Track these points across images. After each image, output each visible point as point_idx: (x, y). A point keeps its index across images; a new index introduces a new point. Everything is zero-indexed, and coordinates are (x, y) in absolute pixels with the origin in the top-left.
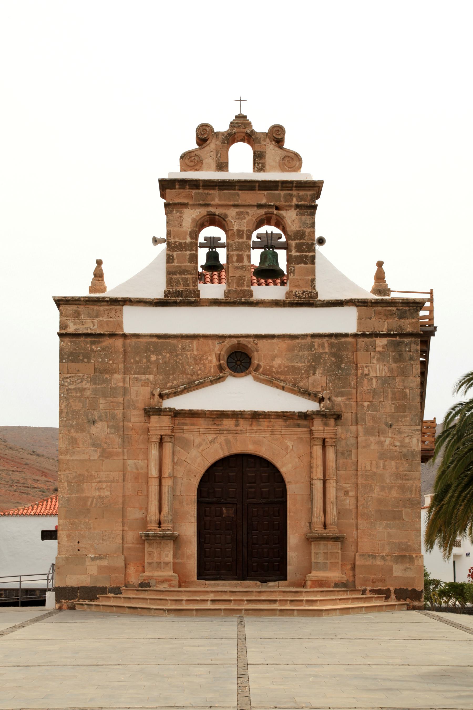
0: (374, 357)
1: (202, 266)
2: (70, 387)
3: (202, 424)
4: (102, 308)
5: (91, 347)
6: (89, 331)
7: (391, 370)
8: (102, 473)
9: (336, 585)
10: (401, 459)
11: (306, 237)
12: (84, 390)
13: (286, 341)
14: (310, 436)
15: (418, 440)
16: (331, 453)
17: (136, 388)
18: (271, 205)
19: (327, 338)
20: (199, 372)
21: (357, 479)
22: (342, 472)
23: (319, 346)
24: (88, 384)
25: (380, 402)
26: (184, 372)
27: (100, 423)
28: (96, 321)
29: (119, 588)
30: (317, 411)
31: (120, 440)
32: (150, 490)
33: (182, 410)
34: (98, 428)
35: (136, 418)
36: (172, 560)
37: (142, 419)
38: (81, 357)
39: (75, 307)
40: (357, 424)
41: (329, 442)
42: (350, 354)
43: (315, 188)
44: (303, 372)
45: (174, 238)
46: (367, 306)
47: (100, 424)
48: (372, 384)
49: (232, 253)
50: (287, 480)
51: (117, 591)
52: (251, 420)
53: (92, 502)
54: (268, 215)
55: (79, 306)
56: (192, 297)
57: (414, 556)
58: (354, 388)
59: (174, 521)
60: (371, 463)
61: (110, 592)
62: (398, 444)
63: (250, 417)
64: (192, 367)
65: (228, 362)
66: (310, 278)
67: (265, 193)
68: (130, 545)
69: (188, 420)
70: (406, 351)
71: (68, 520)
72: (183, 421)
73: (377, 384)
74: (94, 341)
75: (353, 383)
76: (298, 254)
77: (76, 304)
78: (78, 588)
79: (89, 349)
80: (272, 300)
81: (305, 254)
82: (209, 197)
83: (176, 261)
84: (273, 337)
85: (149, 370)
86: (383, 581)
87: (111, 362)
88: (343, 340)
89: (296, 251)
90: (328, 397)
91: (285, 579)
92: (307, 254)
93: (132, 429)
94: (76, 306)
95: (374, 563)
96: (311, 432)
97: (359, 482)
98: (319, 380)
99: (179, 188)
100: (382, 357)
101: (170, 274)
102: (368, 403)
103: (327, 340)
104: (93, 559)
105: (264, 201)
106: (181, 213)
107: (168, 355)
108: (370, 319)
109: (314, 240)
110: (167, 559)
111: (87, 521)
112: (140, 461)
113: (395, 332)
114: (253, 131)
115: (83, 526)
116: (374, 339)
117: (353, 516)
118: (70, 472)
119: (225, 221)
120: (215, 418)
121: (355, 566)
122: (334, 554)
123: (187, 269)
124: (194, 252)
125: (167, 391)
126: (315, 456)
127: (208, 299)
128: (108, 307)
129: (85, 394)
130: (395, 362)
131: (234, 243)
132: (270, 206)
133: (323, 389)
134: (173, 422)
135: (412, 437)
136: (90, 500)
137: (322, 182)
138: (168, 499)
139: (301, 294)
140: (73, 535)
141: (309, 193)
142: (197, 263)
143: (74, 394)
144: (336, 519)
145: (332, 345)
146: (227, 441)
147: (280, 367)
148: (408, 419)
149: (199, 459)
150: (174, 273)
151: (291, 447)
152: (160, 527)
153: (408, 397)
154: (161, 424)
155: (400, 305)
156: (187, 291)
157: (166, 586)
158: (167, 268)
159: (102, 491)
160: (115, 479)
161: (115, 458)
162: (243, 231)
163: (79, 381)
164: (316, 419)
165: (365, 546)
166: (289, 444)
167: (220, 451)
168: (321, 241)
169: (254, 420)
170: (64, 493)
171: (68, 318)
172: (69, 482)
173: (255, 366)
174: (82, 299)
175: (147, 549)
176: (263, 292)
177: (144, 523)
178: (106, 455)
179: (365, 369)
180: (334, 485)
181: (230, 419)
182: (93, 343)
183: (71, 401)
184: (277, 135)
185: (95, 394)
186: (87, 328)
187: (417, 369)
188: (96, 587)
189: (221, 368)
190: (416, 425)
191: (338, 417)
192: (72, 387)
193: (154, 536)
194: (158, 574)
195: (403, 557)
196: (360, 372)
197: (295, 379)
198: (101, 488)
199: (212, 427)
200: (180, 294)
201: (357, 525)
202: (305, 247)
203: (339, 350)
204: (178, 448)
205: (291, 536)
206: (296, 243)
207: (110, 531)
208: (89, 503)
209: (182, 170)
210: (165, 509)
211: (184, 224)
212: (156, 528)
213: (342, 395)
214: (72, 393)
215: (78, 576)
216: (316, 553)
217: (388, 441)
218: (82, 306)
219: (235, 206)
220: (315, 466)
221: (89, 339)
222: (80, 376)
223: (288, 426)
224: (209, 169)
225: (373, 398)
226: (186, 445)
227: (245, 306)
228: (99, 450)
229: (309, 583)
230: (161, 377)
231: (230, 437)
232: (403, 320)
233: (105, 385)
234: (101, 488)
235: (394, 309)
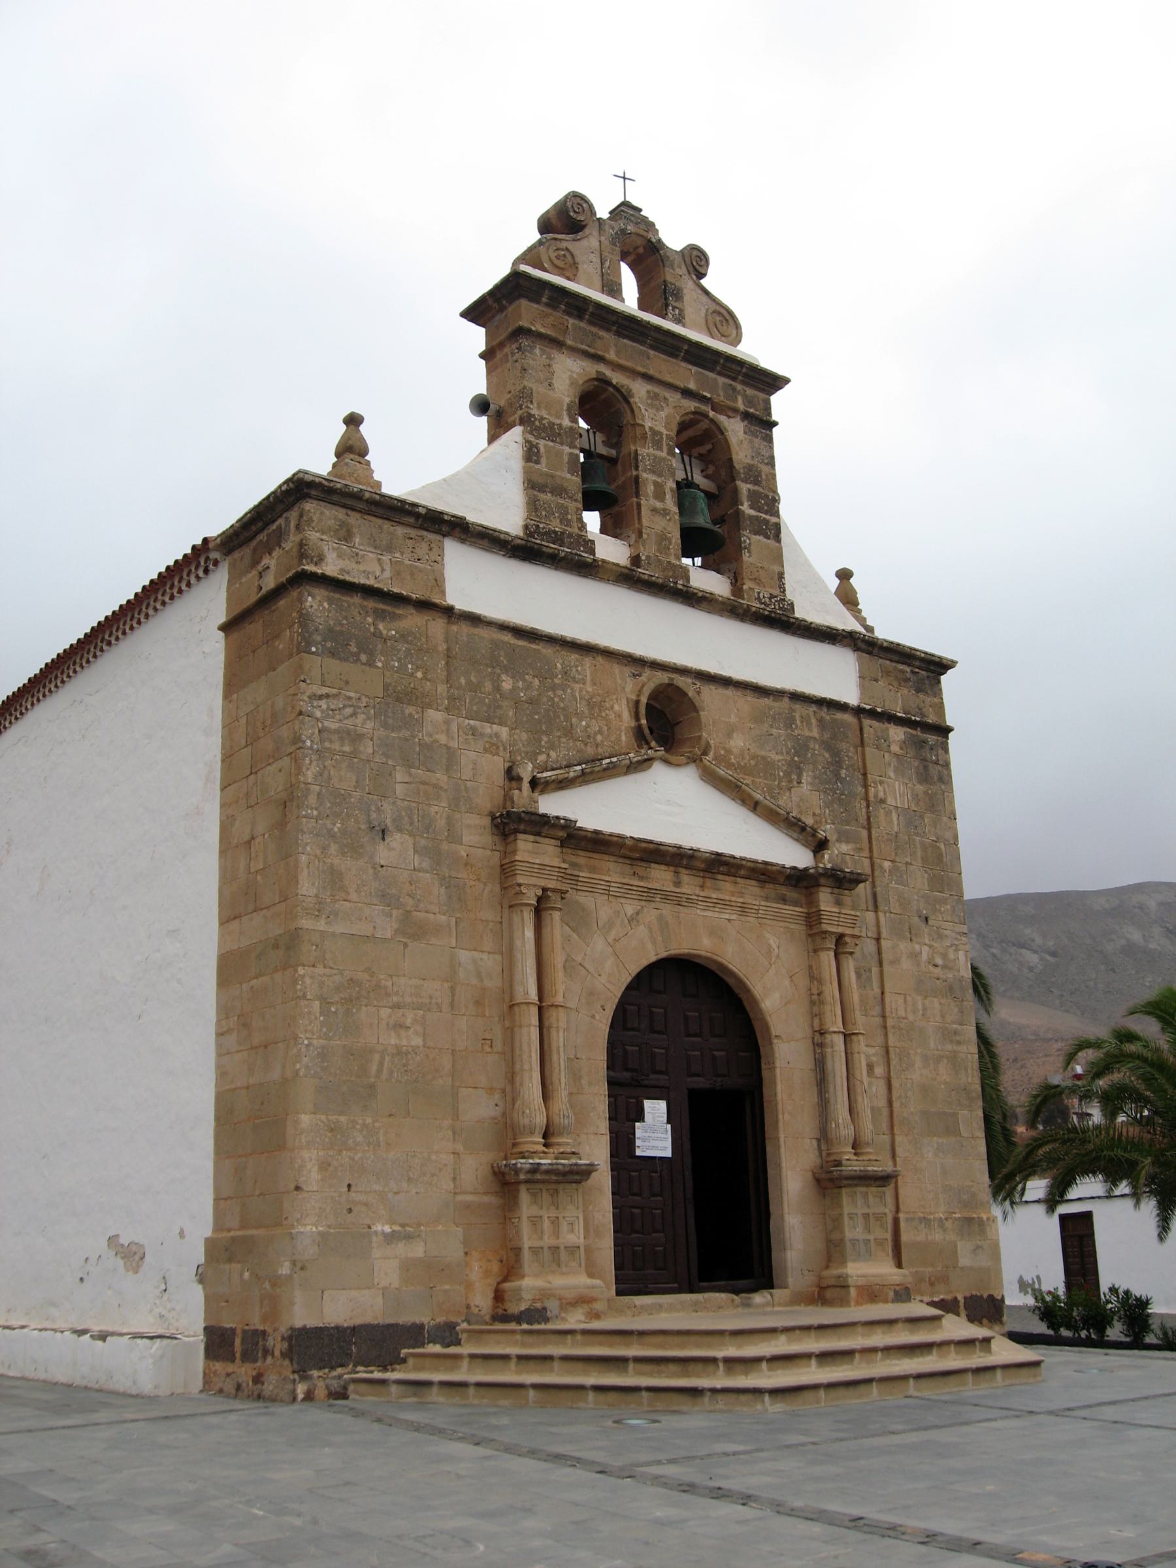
2: (326, 724)
3: (612, 871)
4: (400, 531)
5: (376, 628)
6: (371, 582)
7: (916, 797)
8: (402, 980)
13: (749, 699)
18: (705, 397)
19: (814, 708)
20: (599, 738)
21: (886, 1035)
24: (370, 725)
26: (569, 732)
27: (398, 836)
28: (386, 558)
29: (451, 1327)
31: (443, 890)
34: (393, 849)
35: (475, 836)
39: (340, 513)
40: (876, 909)
45: (539, 407)
46: (870, 653)
47: (397, 840)
49: (645, 475)
51: (448, 1334)
53: (381, 1064)
55: (350, 512)
57: (985, 1218)
61: (433, 1341)
62: (939, 961)
67: (694, 369)
68: (469, 1198)
71: (323, 1117)
73: (898, 824)
74: (383, 611)
76: (753, 512)
77: (344, 506)
78: (354, 1329)
82: (599, 341)
83: (544, 461)
84: (726, 682)
85: (499, 712)
86: (945, 1279)
92: (767, 517)
93: (466, 864)
94: (344, 511)
95: (930, 1238)
97: (890, 1044)
98: (804, 797)
99: (547, 305)
104: (390, 1238)
105: (692, 386)
107: (536, 682)
108: (876, 680)
111: (369, 1121)
112: (485, 956)
115: (360, 1139)
118: (327, 970)
119: (628, 402)
123: (566, 484)
128: (413, 533)
129: (362, 748)
130: (920, 782)
131: (648, 455)
132: (703, 399)
135: (956, 950)
136: (377, 1057)
140: (335, 1163)
143: (336, 746)
147: (742, 755)
158: (527, 473)
159: (403, 1033)
160: (434, 1001)
161: (433, 941)
162: (661, 434)
163: (349, 711)
166: (771, 942)
167: (650, 946)
169: (708, 875)
170: (312, 1032)
171: (324, 537)
172: (325, 1002)
178: (413, 930)
181: (663, 867)
182: (380, 615)
183: (328, 763)
185: (384, 754)
186: (367, 574)
188: (397, 1325)
189: (640, 737)
192: (334, 726)
195: (969, 1220)
196: (872, 791)
198: (401, 1026)
200: (558, 538)
203: (834, 737)
205: (789, 1173)
207: (425, 1155)
208: (374, 1068)
211: (557, 383)
213: (847, 842)
214: (331, 741)
215: (354, 1293)
217: (925, 953)
218: (358, 515)
219: (648, 378)
221: (371, 604)
222: (350, 698)
223: (767, 899)
226: (580, 922)
227: (676, 600)
228: (395, 912)
230: (524, 736)
231: (667, 910)
232: (921, 696)
234: (401, 1026)
235: (908, 669)
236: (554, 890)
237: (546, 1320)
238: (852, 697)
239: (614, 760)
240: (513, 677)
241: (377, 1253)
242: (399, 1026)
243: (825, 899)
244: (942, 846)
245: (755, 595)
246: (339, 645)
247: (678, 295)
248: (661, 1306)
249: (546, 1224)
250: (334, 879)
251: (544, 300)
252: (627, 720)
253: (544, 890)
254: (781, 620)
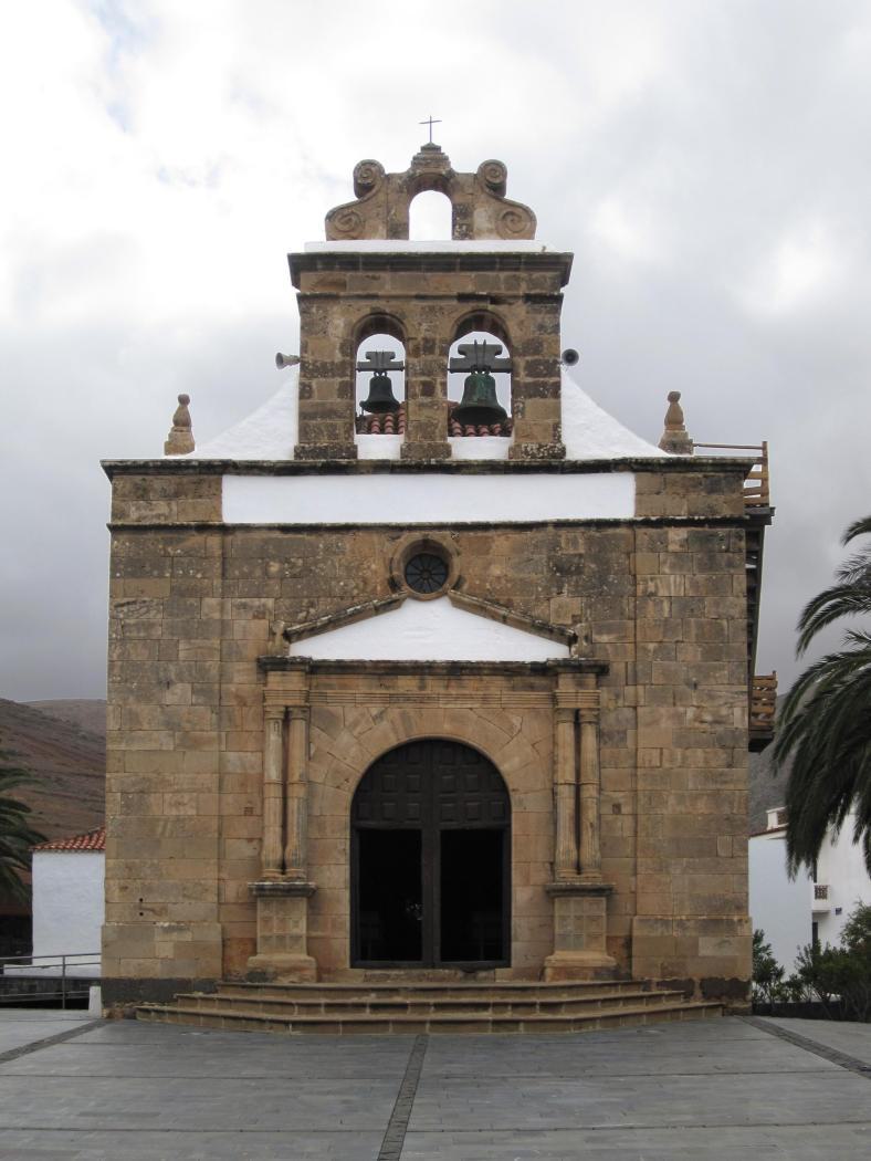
0: (665, 562)
1: (362, 404)
2: (127, 621)
3: (361, 686)
6: (162, 521)
7: (695, 585)
8: (182, 776)
10: (714, 746)
11: (545, 351)
12: (152, 625)
14: (551, 706)
15: (743, 711)
17: (243, 622)
18: (482, 296)
19: (582, 529)
22: (608, 771)
23: (567, 543)
24: (160, 616)
25: (677, 642)
27: (180, 685)
30: (565, 660)
32: (267, 805)
33: (324, 661)
35: (242, 677)
36: (304, 932)
37: (254, 677)
38: (148, 568)
41: (587, 716)
42: (623, 556)
43: (558, 266)
44: (540, 589)
45: (313, 354)
47: (179, 688)
48: (662, 609)
49: (414, 379)
50: (511, 787)
51: (209, 986)
52: (446, 677)
53: (165, 827)
54: (478, 313)
56: (344, 458)
57: (736, 918)
58: (630, 619)
59: (308, 863)
60: (661, 754)
62: (708, 718)
63: (445, 671)
64: (342, 584)
65: (406, 574)
66: (550, 421)
67: (473, 274)
69: (334, 680)
70: (721, 551)
72: (327, 681)
73: (671, 611)
74: (171, 538)
75: (628, 609)
76: (529, 380)
78: (142, 981)
79: (162, 552)
80: (485, 461)
81: (542, 379)
85: (266, 589)
87: (199, 576)
88: (610, 531)
89: (527, 375)
90: (584, 633)
91: (509, 966)
92: (546, 379)
95: (666, 934)
96: (554, 699)
99: (324, 269)
100: (679, 560)
101: (305, 418)
102: (656, 645)
103: (583, 533)
105: (470, 289)
106: (326, 311)
108: (658, 493)
109: (558, 355)
110: (295, 931)
111: (156, 861)
112: (249, 754)
113: (702, 518)
114: (452, 174)
116: (666, 529)
117: (629, 851)
119: (402, 323)
120: (382, 674)
122: (593, 919)
123: (335, 408)
124: (347, 379)
125: (298, 626)
126: (560, 740)
127: (371, 461)
128: (195, 478)
129: (153, 633)
130: (702, 568)
133: (576, 620)
134: (308, 683)
136: (162, 823)
137: (570, 256)
138: (298, 823)
139: (535, 451)
141: (549, 274)
142: (353, 397)
143: (134, 634)
144: (599, 855)
145: (590, 541)
146: (404, 716)
148: (726, 672)
149: (354, 749)
150: (313, 416)
151: (518, 725)
152: (283, 873)
153: (726, 633)
154: (285, 687)
155: (709, 469)
156: (332, 448)
157: (295, 980)
158: (301, 407)
159: (181, 808)
161: (206, 748)
164: (563, 675)
165: (650, 904)
166: (514, 721)
168: (571, 357)
169: (452, 677)
173: (455, 579)
174: (151, 464)
175: (261, 912)
176: (468, 448)
177: (257, 865)
178: (190, 743)
179: (650, 583)
180: (595, 794)
181: (409, 677)
182: (168, 542)
184: (492, 179)
186: (158, 516)
187: (741, 583)
189: (393, 585)
190: (740, 684)
191: (602, 670)
192: (132, 621)
193: (274, 889)
194: (280, 958)
195: (717, 922)
196: (640, 588)
197: (526, 603)
199: (378, 692)
200: (323, 452)
201: (635, 866)
202: (542, 372)
204: (315, 731)
206: (527, 362)
209: (330, 238)
210: (293, 841)
211: (331, 330)
212: (277, 875)
213: (609, 633)
215: (141, 961)
216: (563, 918)
217: (690, 713)
220: (561, 759)
222: (144, 602)
223: (513, 688)
225: (664, 637)
226: (331, 723)
229: (549, 972)
231: (409, 708)
232: (715, 496)
233: (189, 617)
235: (700, 475)
236: (295, 707)
239: (359, 607)
240: (281, 562)
241: (157, 938)
242: (179, 804)
243: (566, 685)
249: (275, 922)
251: (319, 266)
253: (287, 707)
254: (554, 464)
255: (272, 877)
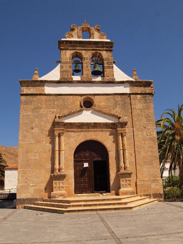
7: (143, 106)
9: (131, 194)
16: (125, 138)
40: (133, 127)
76: (107, 65)
98: (117, 111)
121: (136, 185)
127: (76, 81)
130: (145, 103)
178: (38, 141)
189: (81, 107)
217: (145, 133)
224: (75, 38)
236: (60, 133)
237: (55, 198)
238: (128, 92)
244: (150, 114)
245: (107, 79)
246: (26, 103)
247: (93, 34)
248: (83, 195)
249: (58, 184)
250: (25, 136)
251: (65, 43)
252: (79, 104)
254: (112, 82)
255: (57, 173)
